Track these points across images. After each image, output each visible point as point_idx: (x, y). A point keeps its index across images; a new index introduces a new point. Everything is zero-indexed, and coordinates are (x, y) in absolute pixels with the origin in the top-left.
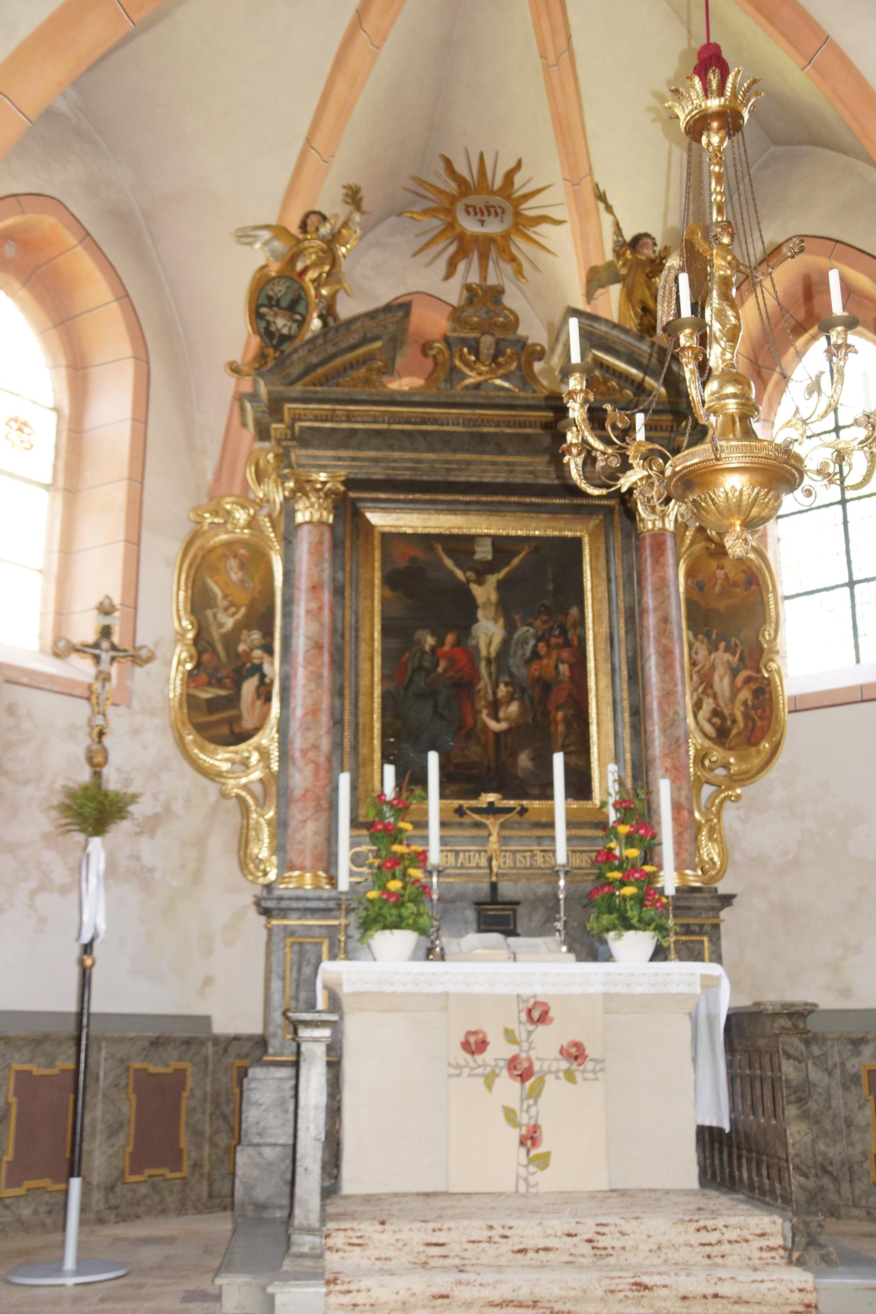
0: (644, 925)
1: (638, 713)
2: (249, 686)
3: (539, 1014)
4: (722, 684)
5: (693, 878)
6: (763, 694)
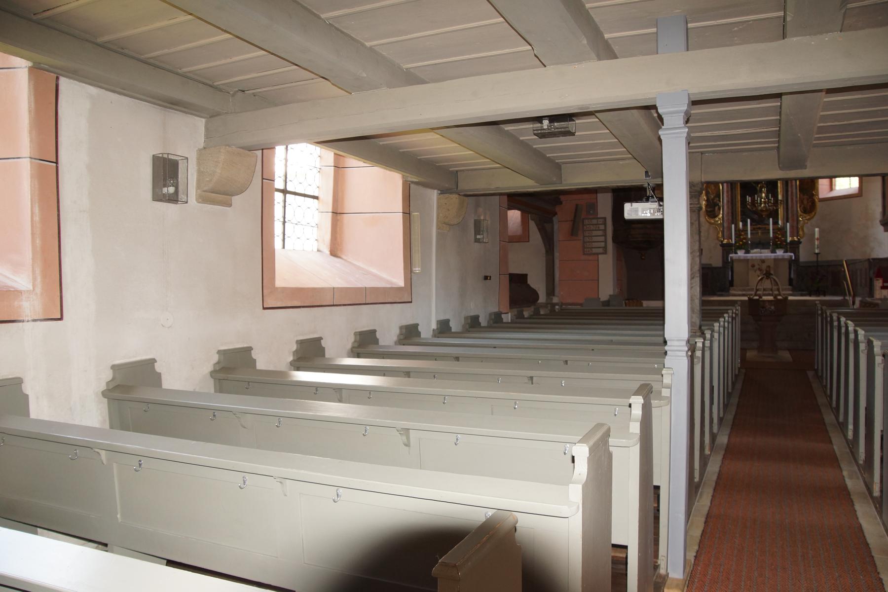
0: (781, 248)
1: (787, 209)
2: (717, 208)
3: (763, 261)
4: (805, 202)
5: (795, 239)
6: (813, 204)
